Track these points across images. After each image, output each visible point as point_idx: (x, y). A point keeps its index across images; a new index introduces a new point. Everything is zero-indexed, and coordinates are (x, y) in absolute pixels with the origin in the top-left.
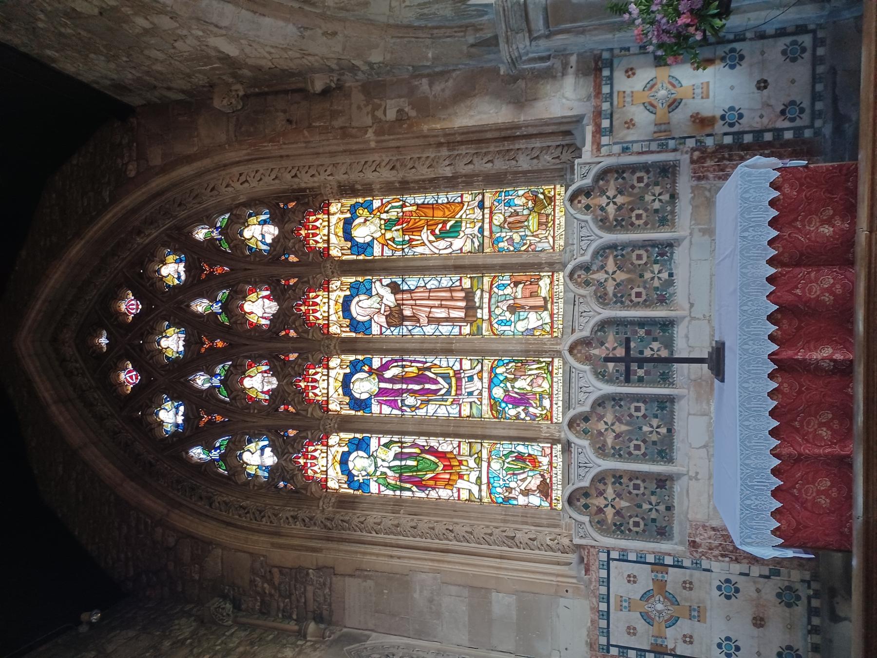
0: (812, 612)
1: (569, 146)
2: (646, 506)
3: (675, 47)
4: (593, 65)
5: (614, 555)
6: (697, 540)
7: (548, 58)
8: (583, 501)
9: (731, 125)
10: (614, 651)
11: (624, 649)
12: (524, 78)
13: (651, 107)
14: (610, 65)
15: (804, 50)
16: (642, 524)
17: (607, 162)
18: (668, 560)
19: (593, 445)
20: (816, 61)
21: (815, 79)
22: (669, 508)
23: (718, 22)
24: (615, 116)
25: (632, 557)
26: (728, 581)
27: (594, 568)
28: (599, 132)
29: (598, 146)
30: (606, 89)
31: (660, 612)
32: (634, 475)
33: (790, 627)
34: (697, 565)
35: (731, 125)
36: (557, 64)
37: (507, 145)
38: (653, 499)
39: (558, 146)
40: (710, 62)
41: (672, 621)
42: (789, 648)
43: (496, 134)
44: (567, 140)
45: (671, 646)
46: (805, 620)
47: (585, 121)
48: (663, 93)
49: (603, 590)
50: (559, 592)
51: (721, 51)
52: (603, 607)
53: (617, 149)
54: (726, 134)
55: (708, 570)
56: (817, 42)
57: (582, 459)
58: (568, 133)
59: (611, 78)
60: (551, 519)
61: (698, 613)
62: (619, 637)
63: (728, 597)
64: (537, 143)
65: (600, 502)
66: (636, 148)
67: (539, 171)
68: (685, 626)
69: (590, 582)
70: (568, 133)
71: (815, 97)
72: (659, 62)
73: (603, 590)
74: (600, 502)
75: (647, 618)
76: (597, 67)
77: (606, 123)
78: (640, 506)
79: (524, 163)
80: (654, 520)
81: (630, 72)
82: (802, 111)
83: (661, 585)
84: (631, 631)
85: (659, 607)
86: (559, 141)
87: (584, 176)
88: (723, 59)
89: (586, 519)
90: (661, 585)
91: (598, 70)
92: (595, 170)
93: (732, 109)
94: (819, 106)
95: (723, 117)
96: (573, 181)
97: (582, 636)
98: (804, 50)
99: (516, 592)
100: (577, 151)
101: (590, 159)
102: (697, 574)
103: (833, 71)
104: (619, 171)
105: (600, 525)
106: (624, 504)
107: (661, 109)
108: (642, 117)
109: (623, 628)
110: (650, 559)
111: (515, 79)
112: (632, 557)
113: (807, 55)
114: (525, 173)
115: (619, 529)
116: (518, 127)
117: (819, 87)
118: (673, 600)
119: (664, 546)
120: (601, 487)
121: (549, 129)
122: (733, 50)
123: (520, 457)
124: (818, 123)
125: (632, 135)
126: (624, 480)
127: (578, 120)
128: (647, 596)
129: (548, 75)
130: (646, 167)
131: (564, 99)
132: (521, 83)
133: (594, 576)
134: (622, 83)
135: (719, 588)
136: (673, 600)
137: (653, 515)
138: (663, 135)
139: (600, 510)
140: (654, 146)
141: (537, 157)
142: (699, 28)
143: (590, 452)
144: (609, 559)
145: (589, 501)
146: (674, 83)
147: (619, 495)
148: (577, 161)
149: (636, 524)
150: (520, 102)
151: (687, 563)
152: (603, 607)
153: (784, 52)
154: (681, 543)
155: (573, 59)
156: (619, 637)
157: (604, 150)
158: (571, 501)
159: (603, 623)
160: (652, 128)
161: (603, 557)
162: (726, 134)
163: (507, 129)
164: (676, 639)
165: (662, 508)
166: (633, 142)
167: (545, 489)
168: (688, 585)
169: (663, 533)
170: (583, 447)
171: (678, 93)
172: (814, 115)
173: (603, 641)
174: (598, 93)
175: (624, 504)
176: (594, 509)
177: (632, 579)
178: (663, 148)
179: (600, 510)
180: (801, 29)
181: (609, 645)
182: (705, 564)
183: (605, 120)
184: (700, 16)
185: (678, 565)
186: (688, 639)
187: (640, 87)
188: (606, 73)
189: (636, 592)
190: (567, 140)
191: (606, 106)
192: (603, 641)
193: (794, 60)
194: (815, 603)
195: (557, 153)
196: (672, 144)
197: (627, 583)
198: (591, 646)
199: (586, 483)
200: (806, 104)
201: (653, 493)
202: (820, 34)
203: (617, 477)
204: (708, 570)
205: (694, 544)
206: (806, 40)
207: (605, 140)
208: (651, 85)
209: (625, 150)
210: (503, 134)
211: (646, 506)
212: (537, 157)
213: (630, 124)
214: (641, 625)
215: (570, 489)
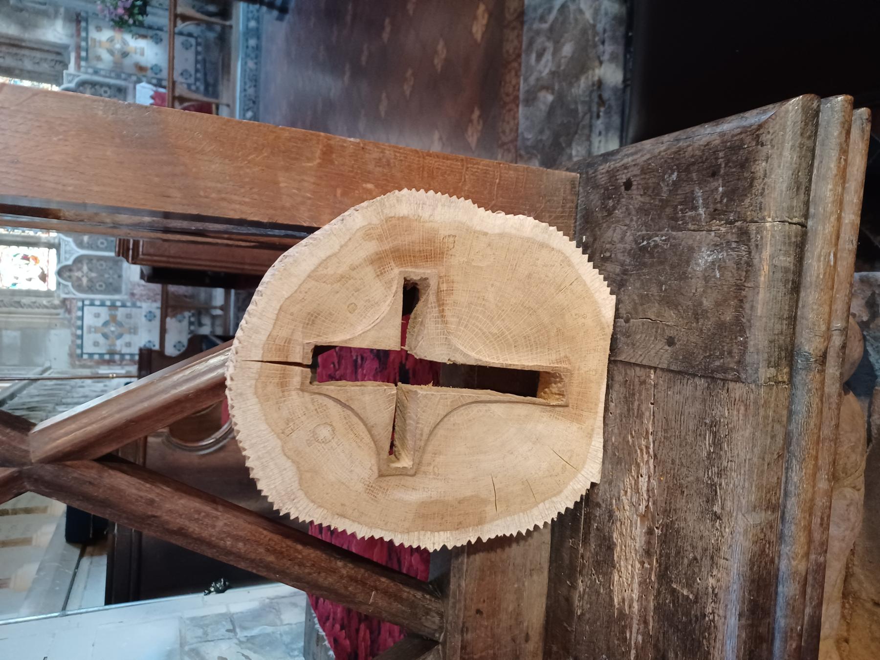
0: (191, 323)
1: (61, 62)
2: (106, 276)
3: (120, 24)
4: (75, 17)
5: (87, 302)
6: (135, 291)
7: (45, 4)
8: (68, 274)
9: (156, 74)
10: (85, 357)
11: (91, 355)
12: (27, 11)
13: (111, 52)
14: (87, 21)
15: (191, 46)
16: (104, 286)
17: (84, 77)
18: (118, 304)
19: (75, 241)
20: (197, 53)
21: (197, 62)
22: (120, 276)
23: (140, 18)
24: (89, 52)
25: (97, 303)
26: (150, 312)
27: (74, 310)
28: (79, 58)
29: (78, 67)
30: (83, 34)
31: (113, 332)
32: (100, 258)
33: (180, 332)
34: (134, 305)
35: (156, 74)
36: (51, 10)
37: (14, 50)
38: (111, 272)
39: (52, 60)
40: (144, 37)
41: (120, 336)
42: (179, 342)
43: (7, 41)
44: (59, 58)
45: (118, 348)
46: (187, 328)
47: (70, 49)
48: (118, 46)
49: (79, 323)
50: (50, 327)
51: (151, 33)
52: (79, 332)
53: (90, 70)
54: (153, 78)
55: (140, 307)
56: (198, 44)
57: (68, 248)
58: (58, 54)
59: (86, 30)
60: (48, 294)
61: (134, 330)
62: (88, 348)
63: (150, 320)
64: (38, 55)
65: (79, 274)
66: (102, 73)
67: (40, 74)
68: (127, 338)
69: (71, 319)
70: (58, 54)
71: (197, 71)
72: (113, 28)
73: (79, 323)
74: (79, 274)
75: (105, 336)
76: (78, 20)
77: (83, 54)
78: (102, 276)
79: (28, 65)
80: (111, 284)
81: (99, 29)
82: (191, 76)
83: (113, 318)
84: (96, 344)
85: (113, 329)
86: (53, 57)
87: (70, 82)
88: (152, 37)
89: (69, 284)
90: (113, 318)
91: (78, 22)
92: (76, 80)
93: (156, 65)
94: (199, 75)
95: (152, 69)
96: (62, 84)
97: (66, 349)
98: (191, 46)
99: (20, 329)
100: (66, 66)
101: (73, 72)
102: (134, 310)
103: (204, 60)
104: (93, 84)
105: (79, 288)
106: (93, 275)
107: (118, 55)
108: (106, 56)
109: (91, 343)
110: (108, 303)
111: (21, 10)
112: (97, 303)
113: (193, 49)
114: (29, 72)
115: (90, 289)
116: (22, 40)
117: (199, 66)
118: (120, 325)
119: (116, 297)
120: (79, 265)
121: (46, 48)
122: (156, 35)
123: (25, 258)
124: (198, 84)
125: (100, 66)
126: (94, 261)
127: (66, 47)
128: (106, 324)
129: (45, 14)
130: (109, 86)
131: (56, 32)
132: (25, 14)
133: (74, 315)
134: (94, 34)
135: (146, 316)
136: (120, 325)
137: (111, 280)
138: (117, 70)
139: (79, 279)
140: (113, 75)
141: (38, 63)
142: (132, 16)
143: (73, 245)
144: (83, 305)
145: (72, 274)
146: (125, 43)
147: (90, 270)
148: (65, 72)
149: (101, 286)
150: (24, 25)
151: (129, 304)
152: (79, 332)
153: (183, 44)
154: (126, 294)
155: (62, 10)
156: (88, 348)
157: (82, 69)
158: (60, 273)
159: (79, 342)
160: (112, 65)
161: (80, 304)
162: (153, 78)
163: (15, 39)
164: (121, 346)
165: (116, 276)
166: (101, 69)
167: (43, 277)
168: (129, 316)
169: (117, 290)
170: (68, 242)
171: (127, 49)
172: (196, 79)
173: (79, 351)
174: (79, 35)
175: (93, 275)
176: (74, 279)
177: (97, 316)
178: (118, 77)
179: (79, 279)
180: (190, 35)
181: (82, 354)
182: (138, 304)
183: (84, 53)
184: (130, 11)
185: (124, 306)
186: (128, 345)
187: (105, 39)
188: (83, 24)
189: (99, 323)
190: (59, 58)
191: (83, 44)
192: (79, 351)
193: (187, 49)
194: (192, 319)
195: (53, 64)
196: (123, 76)
197: (93, 317)
198: (71, 355)
199: (70, 262)
200: (193, 72)
201: (111, 268)
202: (200, 40)
203: (90, 259)
204: (140, 307)
205: (133, 295)
206: (193, 41)
207: (83, 63)
208: (111, 40)
209: (96, 72)
210: (12, 42)
211: (106, 276)
212: (38, 63)
213: (99, 58)
214: (102, 340)
215: (60, 266)
